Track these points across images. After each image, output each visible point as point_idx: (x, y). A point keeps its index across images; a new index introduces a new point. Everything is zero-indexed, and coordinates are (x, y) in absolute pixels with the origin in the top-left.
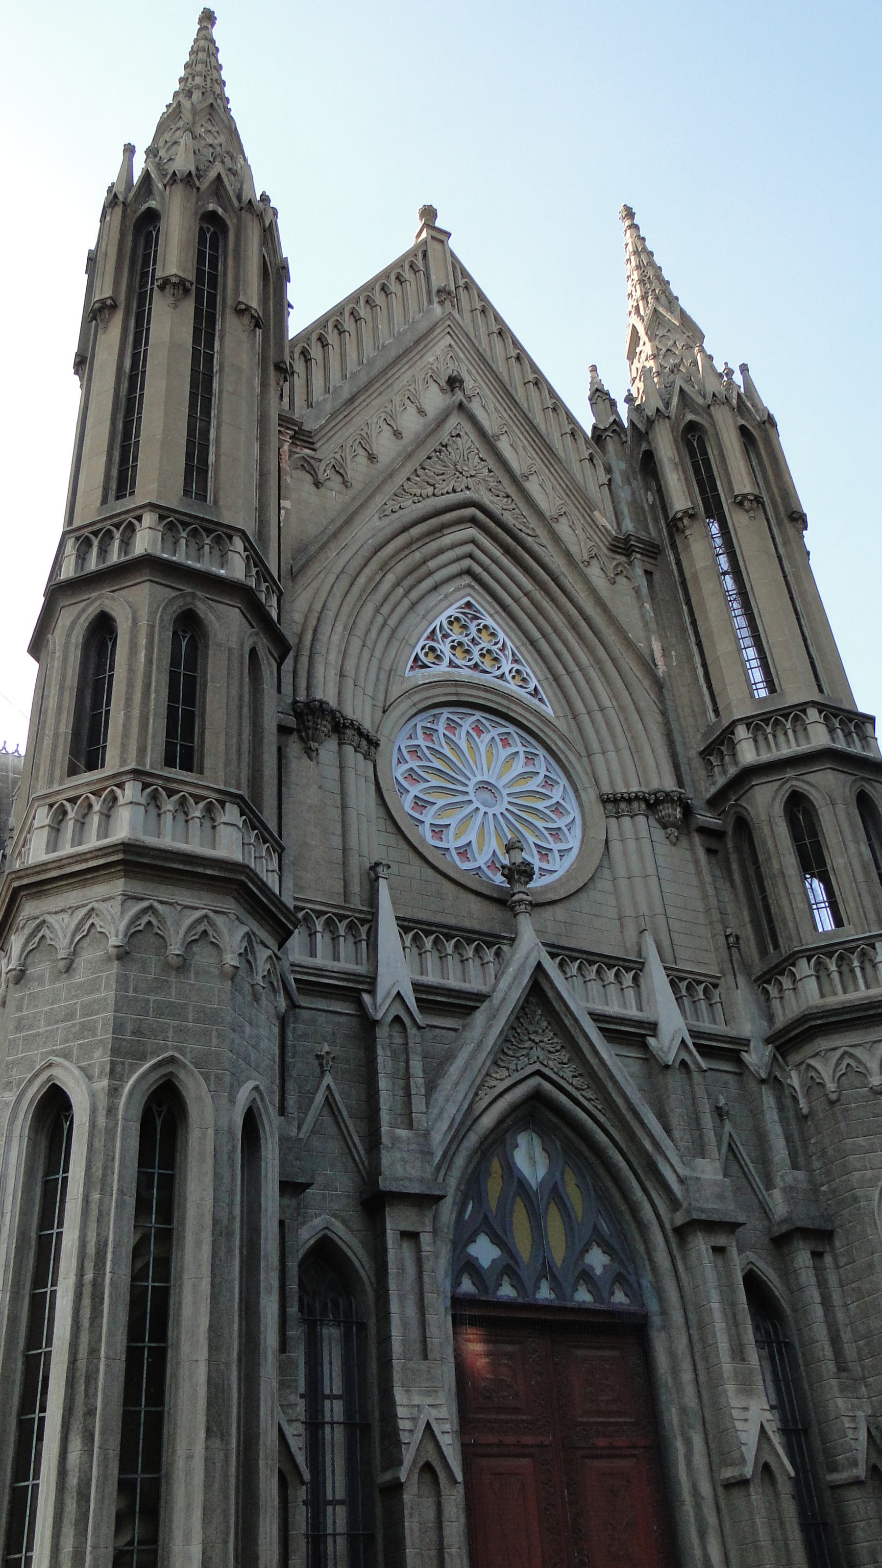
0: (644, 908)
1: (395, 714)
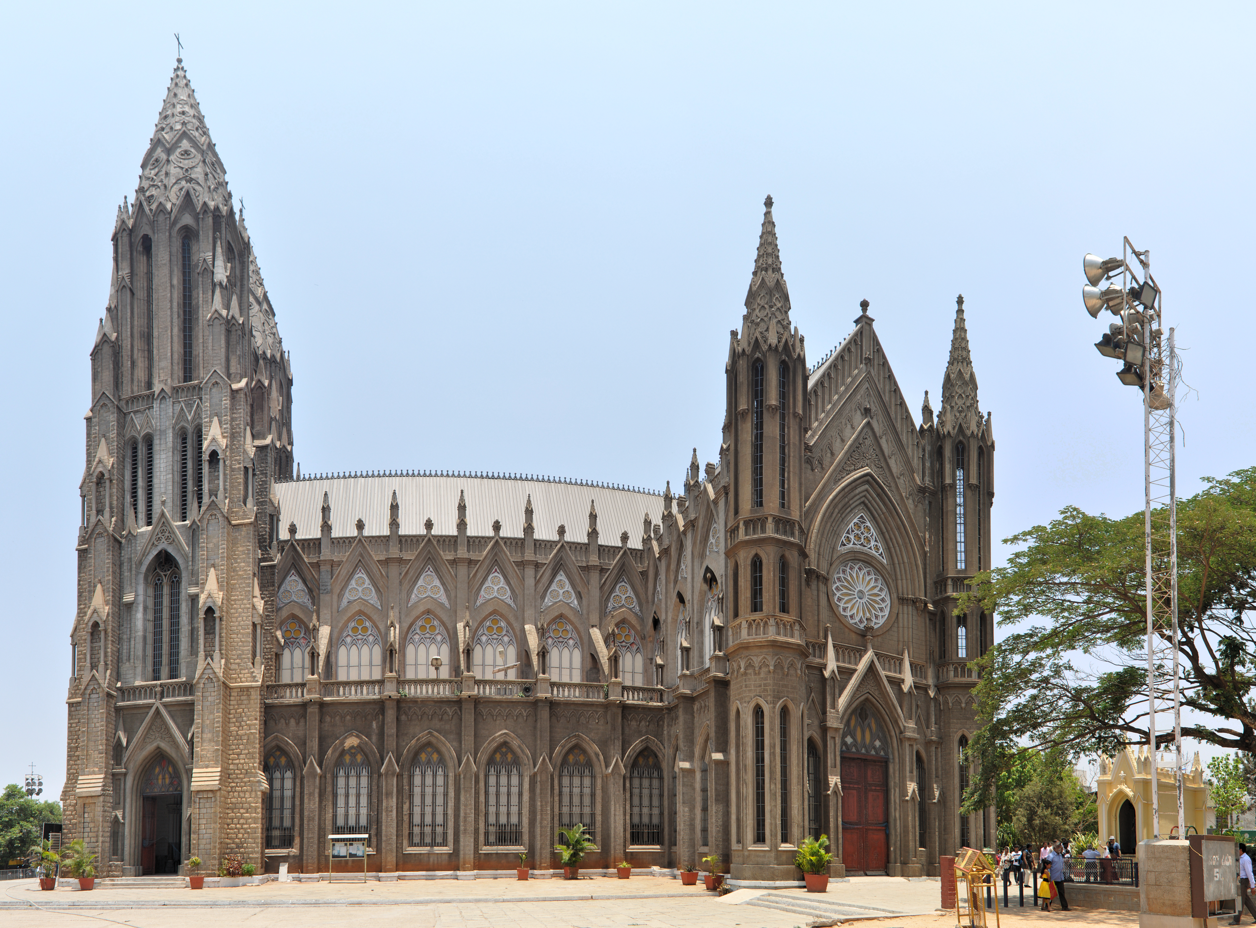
0: (906, 639)
1: (834, 566)
